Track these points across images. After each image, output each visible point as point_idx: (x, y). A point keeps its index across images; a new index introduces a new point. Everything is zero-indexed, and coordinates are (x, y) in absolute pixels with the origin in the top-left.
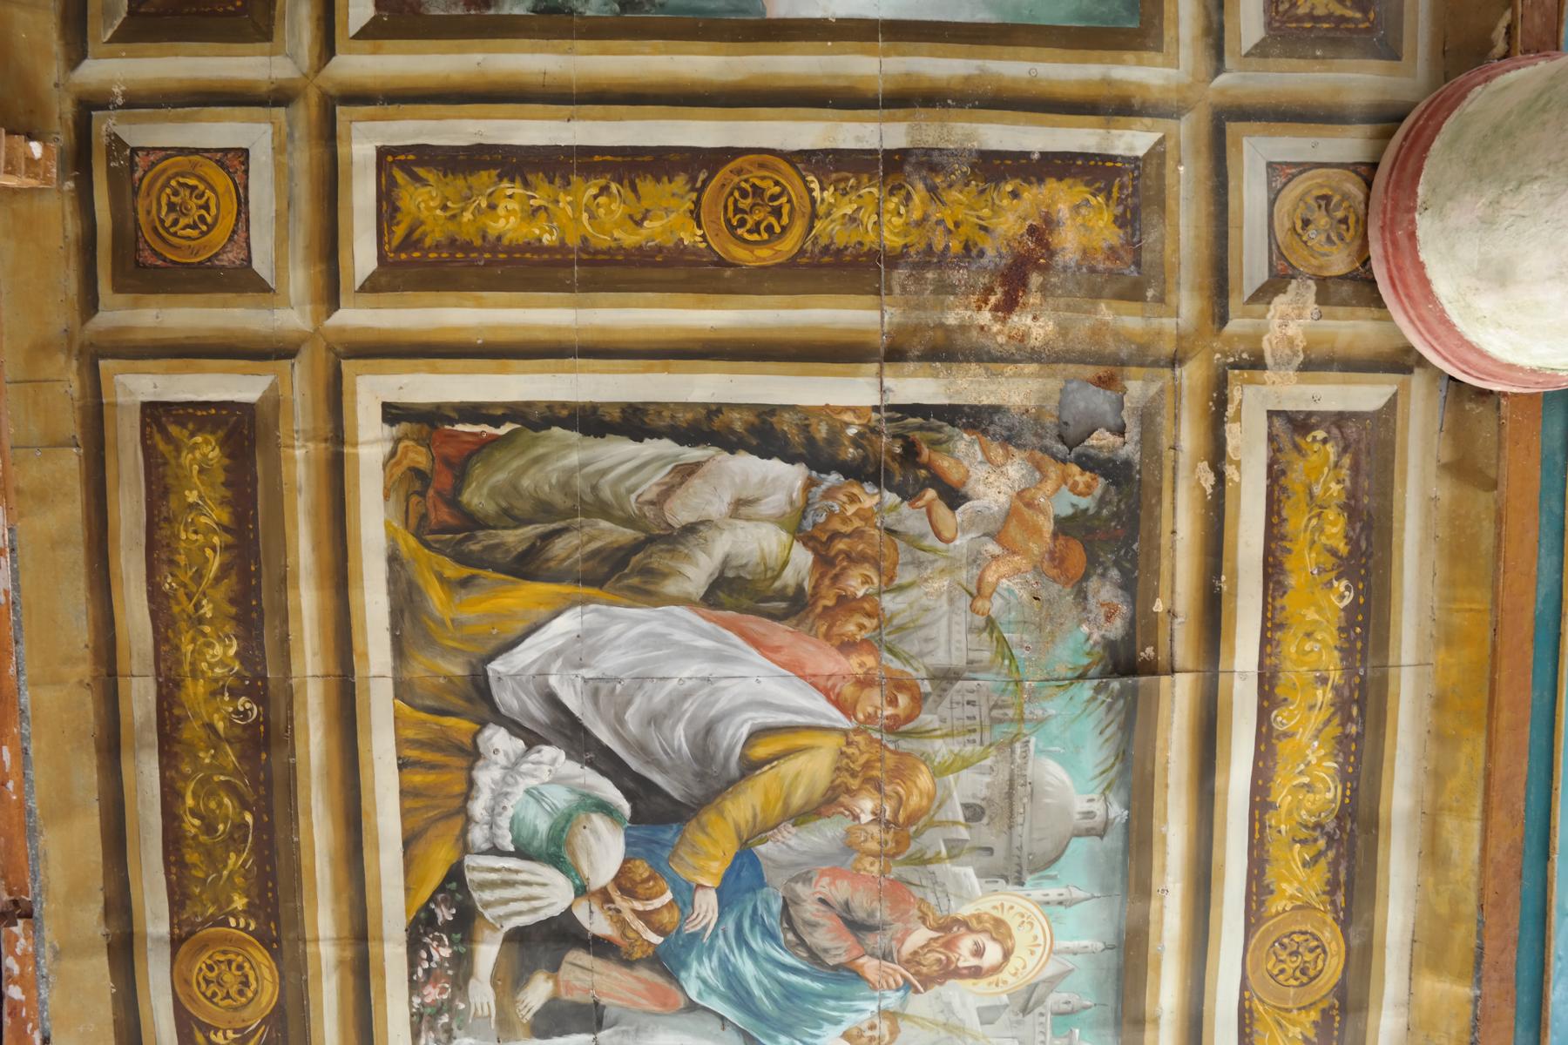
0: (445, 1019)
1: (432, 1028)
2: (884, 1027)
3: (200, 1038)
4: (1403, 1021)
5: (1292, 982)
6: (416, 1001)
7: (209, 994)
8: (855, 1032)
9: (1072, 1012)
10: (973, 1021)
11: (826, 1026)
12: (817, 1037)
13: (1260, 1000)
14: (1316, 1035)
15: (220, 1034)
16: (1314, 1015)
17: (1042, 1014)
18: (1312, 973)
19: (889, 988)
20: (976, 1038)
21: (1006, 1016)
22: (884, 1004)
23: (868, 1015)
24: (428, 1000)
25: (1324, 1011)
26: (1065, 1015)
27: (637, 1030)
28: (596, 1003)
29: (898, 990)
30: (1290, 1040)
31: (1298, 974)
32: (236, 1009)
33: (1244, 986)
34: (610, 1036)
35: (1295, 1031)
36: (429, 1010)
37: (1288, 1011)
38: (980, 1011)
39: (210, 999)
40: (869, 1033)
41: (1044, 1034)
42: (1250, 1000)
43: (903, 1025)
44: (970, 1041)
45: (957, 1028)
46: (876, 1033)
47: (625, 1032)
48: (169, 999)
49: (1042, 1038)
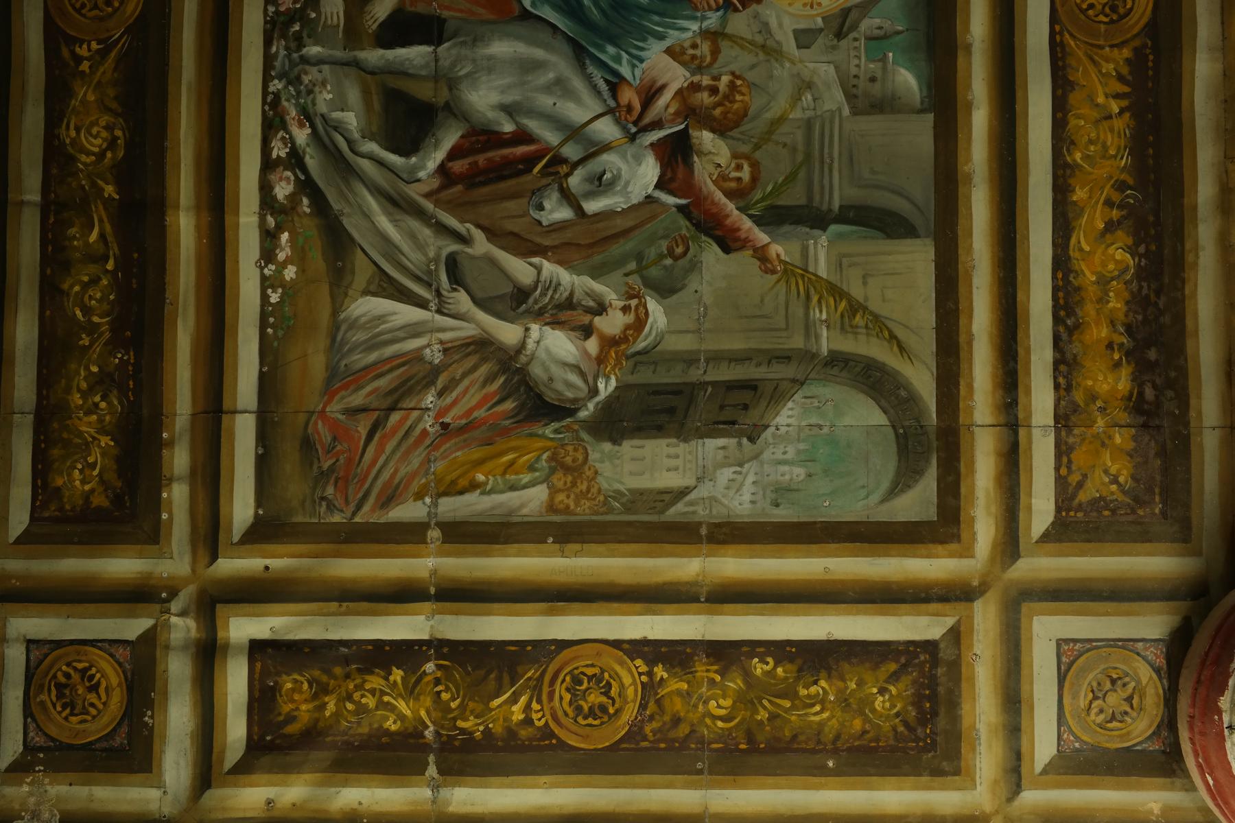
0: (297, 27)
1: (284, 36)
2: (705, 48)
3: (65, 53)
4: (1219, 67)
5: (1102, 18)
6: (271, 9)
7: (78, 5)
8: (678, 49)
9: (885, 37)
10: (790, 46)
11: (651, 40)
12: (642, 49)
13: (1071, 35)
14: (1131, 73)
15: (85, 46)
16: (1126, 53)
17: (856, 39)
18: (1122, 11)
19: (710, 9)
20: (793, 63)
21: (820, 40)
22: (705, 24)
23: (690, 34)
24: (282, 9)
25: (1135, 49)
26: (878, 39)
27: (475, 40)
28: (439, 17)
29: (718, 10)
30: (1103, 75)
31: (1107, 10)
32: (101, 19)
33: (1054, 18)
34: (449, 49)
35: (1109, 67)
36: (282, 19)
37: (1101, 47)
38: (798, 34)
39: (78, 11)
40: (691, 52)
41: (859, 58)
42: (1061, 33)
43: (724, 44)
44: (787, 65)
45: (775, 51)
46: (698, 52)
47: (463, 43)
48: (42, 14)
49: (856, 61)
